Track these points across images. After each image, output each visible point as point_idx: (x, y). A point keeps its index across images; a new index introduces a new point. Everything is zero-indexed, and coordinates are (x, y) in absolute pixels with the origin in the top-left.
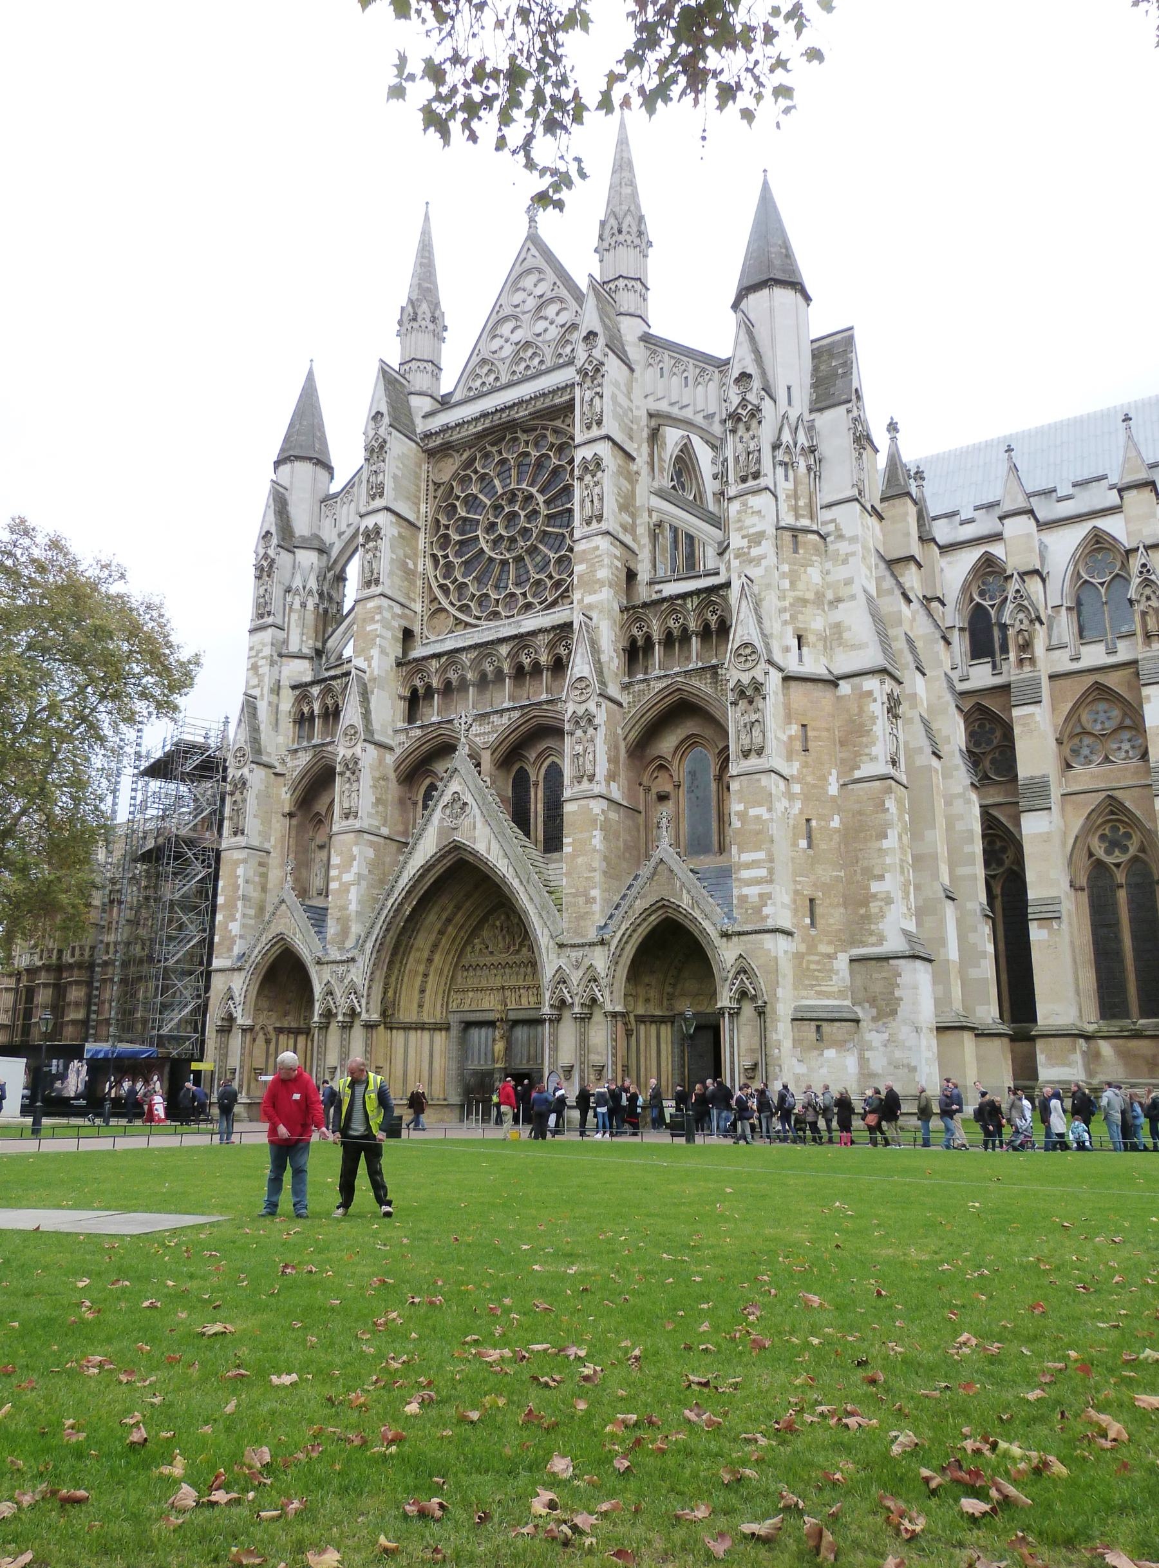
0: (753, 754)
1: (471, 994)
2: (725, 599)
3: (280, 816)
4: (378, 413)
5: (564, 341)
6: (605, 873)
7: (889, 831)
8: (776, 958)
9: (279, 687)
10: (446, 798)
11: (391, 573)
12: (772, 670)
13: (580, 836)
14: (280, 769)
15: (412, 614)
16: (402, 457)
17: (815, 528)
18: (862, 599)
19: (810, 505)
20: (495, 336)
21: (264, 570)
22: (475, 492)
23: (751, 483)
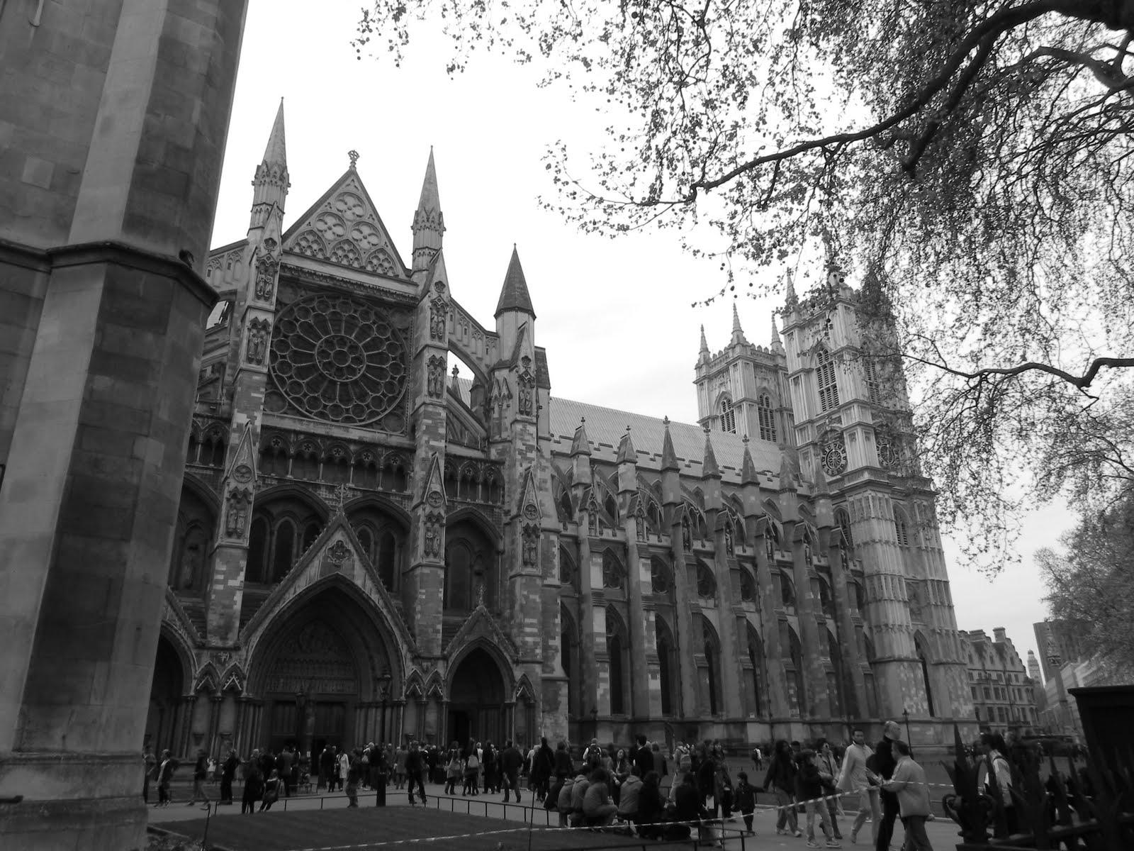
1: (282, 680)
22: (312, 322)
23: (525, 417)
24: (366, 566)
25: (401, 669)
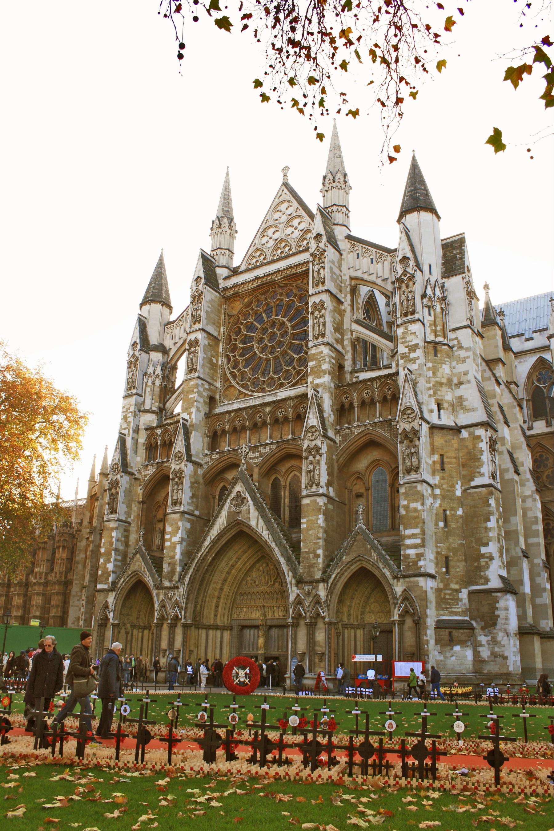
0: (413, 473)
1: (245, 609)
2: (395, 382)
3: (136, 503)
4: (198, 277)
5: (302, 239)
6: (325, 540)
7: (491, 517)
8: (426, 592)
9: (138, 429)
10: (233, 495)
11: (203, 366)
12: (424, 424)
13: (310, 518)
14: (137, 476)
15: (215, 388)
16: (211, 301)
17: (446, 342)
18: (474, 382)
19: (444, 330)
20: (264, 236)
21: (133, 363)
22: (251, 320)
23: (410, 317)
24: (259, 507)
25: (288, 595)
